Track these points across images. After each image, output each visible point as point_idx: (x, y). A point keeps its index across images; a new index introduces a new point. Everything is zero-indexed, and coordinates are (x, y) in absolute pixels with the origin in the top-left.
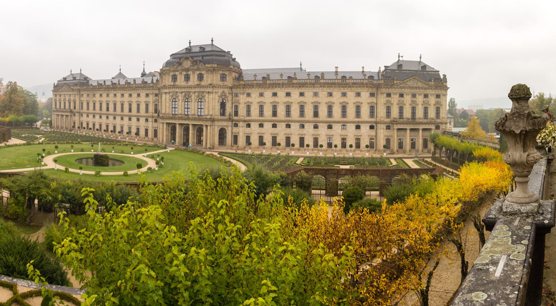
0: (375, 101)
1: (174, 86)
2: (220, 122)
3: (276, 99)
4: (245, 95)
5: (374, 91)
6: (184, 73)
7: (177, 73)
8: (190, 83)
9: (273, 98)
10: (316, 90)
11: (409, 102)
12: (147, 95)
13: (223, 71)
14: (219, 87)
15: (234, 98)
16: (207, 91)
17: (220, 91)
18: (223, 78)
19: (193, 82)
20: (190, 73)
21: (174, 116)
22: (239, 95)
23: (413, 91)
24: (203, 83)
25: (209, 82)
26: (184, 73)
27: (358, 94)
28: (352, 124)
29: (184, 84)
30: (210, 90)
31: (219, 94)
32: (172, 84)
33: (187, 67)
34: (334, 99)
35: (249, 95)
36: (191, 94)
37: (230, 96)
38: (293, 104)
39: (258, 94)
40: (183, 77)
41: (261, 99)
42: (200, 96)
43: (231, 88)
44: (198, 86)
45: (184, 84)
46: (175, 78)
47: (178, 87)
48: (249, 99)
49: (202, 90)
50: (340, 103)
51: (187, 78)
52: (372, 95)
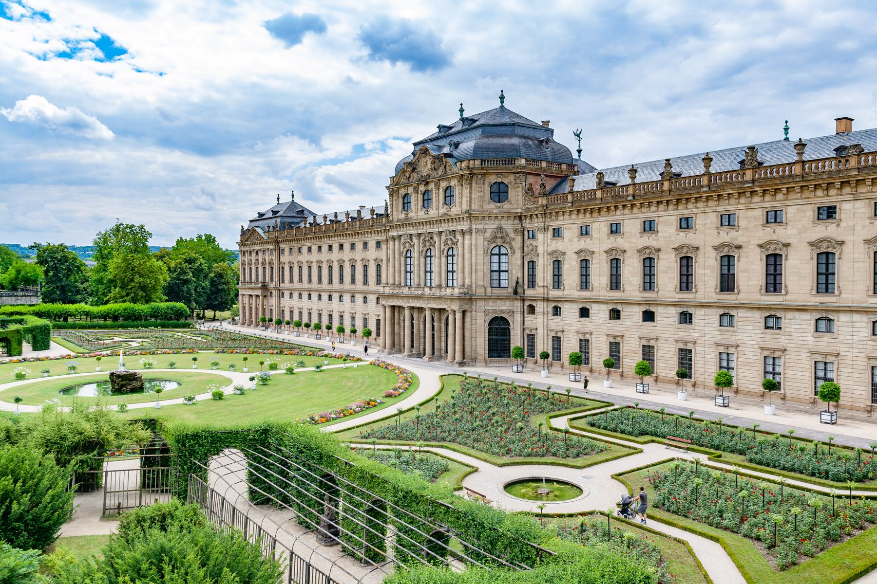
2: (491, 303)
3: (619, 242)
4: (550, 233)
6: (422, 188)
8: (433, 213)
9: (612, 238)
10: (726, 207)
13: (497, 174)
14: (489, 216)
16: (459, 228)
17: (491, 226)
18: (499, 193)
19: (438, 209)
20: (432, 186)
25: (465, 207)
28: (856, 317)
29: (421, 214)
30: (464, 226)
31: (488, 235)
34: (790, 231)
35: (557, 233)
37: (519, 238)
38: (662, 255)
39: (576, 230)
40: (420, 197)
42: (449, 242)
43: (520, 218)
45: (421, 214)
50: (811, 244)
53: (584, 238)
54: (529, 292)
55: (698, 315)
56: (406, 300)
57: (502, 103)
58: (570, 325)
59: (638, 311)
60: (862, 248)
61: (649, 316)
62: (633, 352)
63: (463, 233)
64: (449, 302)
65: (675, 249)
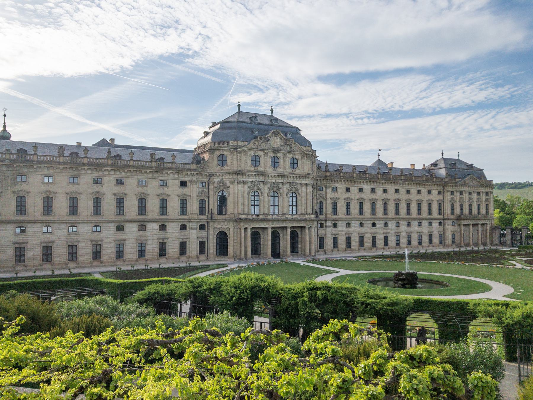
0: (442, 199)
1: (258, 173)
4: (331, 190)
5: (441, 188)
7: (260, 153)
8: (280, 170)
9: (360, 194)
11: (463, 199)
12: (183, 184)
15: (319, 193)
20: (280, 155)
21: (256, 218)
22: (324, 189)
23: (470, 189)
24: (298, 172)
25: (306, 171)
26: (271, 154)
27: (429, 192)
28: (426, 221)
29: (270, 170)
32: (252, 169)
33: (276, 146)
34: (412, 197)
35: (335, 190)
36: (281, 186)
38: (378, 202)
40: (269, 160)
41: (348, 195)
42: (294, 189)
44: (292, 175)
45: (270, 170)
46: (256, 161)
47: (264, 175)
48: (336, 195)
49: (297, 181)
51: (275, 162)
52: (440, 193)
53: (348, 193)
54: (321, 217)
55: (390, 223)
56: (270, 223)
57: (272, 113)
58: (342, 231)
59: (370, 223)
60: (426, 202)
61: (374, 225)
62: (368, 239)
63: (306, 185)
64: (308, 223)
65: (382, 200)
